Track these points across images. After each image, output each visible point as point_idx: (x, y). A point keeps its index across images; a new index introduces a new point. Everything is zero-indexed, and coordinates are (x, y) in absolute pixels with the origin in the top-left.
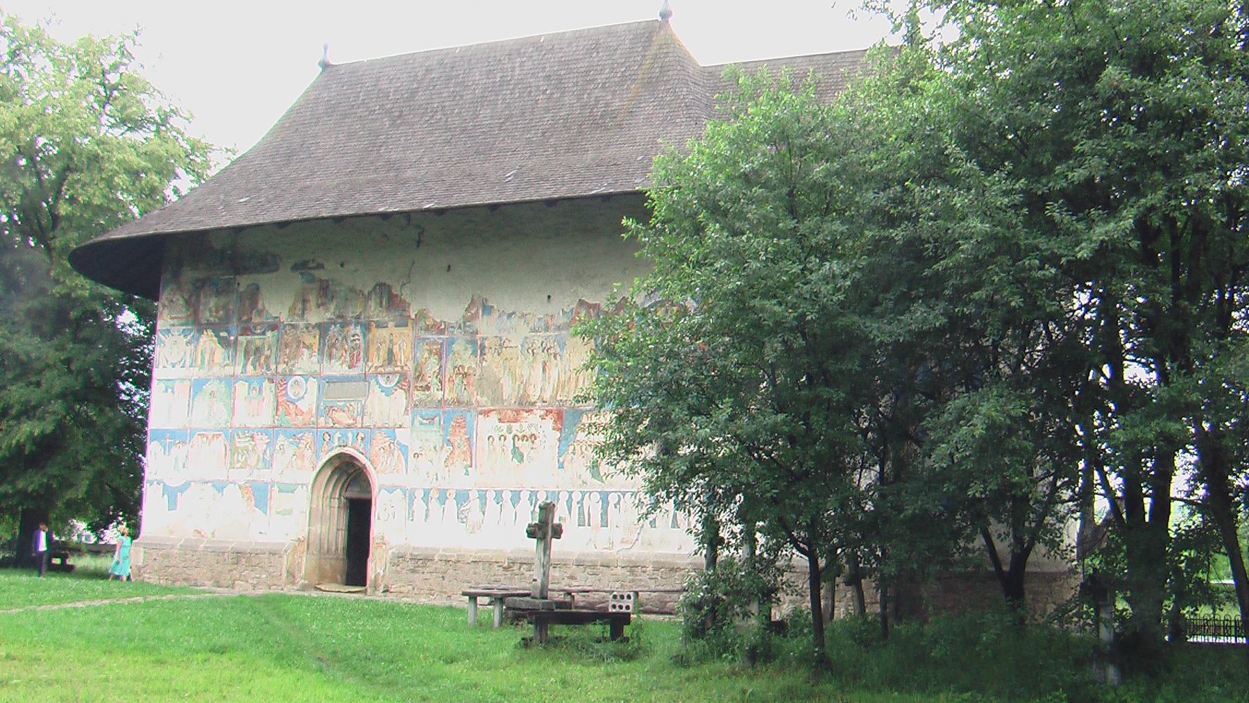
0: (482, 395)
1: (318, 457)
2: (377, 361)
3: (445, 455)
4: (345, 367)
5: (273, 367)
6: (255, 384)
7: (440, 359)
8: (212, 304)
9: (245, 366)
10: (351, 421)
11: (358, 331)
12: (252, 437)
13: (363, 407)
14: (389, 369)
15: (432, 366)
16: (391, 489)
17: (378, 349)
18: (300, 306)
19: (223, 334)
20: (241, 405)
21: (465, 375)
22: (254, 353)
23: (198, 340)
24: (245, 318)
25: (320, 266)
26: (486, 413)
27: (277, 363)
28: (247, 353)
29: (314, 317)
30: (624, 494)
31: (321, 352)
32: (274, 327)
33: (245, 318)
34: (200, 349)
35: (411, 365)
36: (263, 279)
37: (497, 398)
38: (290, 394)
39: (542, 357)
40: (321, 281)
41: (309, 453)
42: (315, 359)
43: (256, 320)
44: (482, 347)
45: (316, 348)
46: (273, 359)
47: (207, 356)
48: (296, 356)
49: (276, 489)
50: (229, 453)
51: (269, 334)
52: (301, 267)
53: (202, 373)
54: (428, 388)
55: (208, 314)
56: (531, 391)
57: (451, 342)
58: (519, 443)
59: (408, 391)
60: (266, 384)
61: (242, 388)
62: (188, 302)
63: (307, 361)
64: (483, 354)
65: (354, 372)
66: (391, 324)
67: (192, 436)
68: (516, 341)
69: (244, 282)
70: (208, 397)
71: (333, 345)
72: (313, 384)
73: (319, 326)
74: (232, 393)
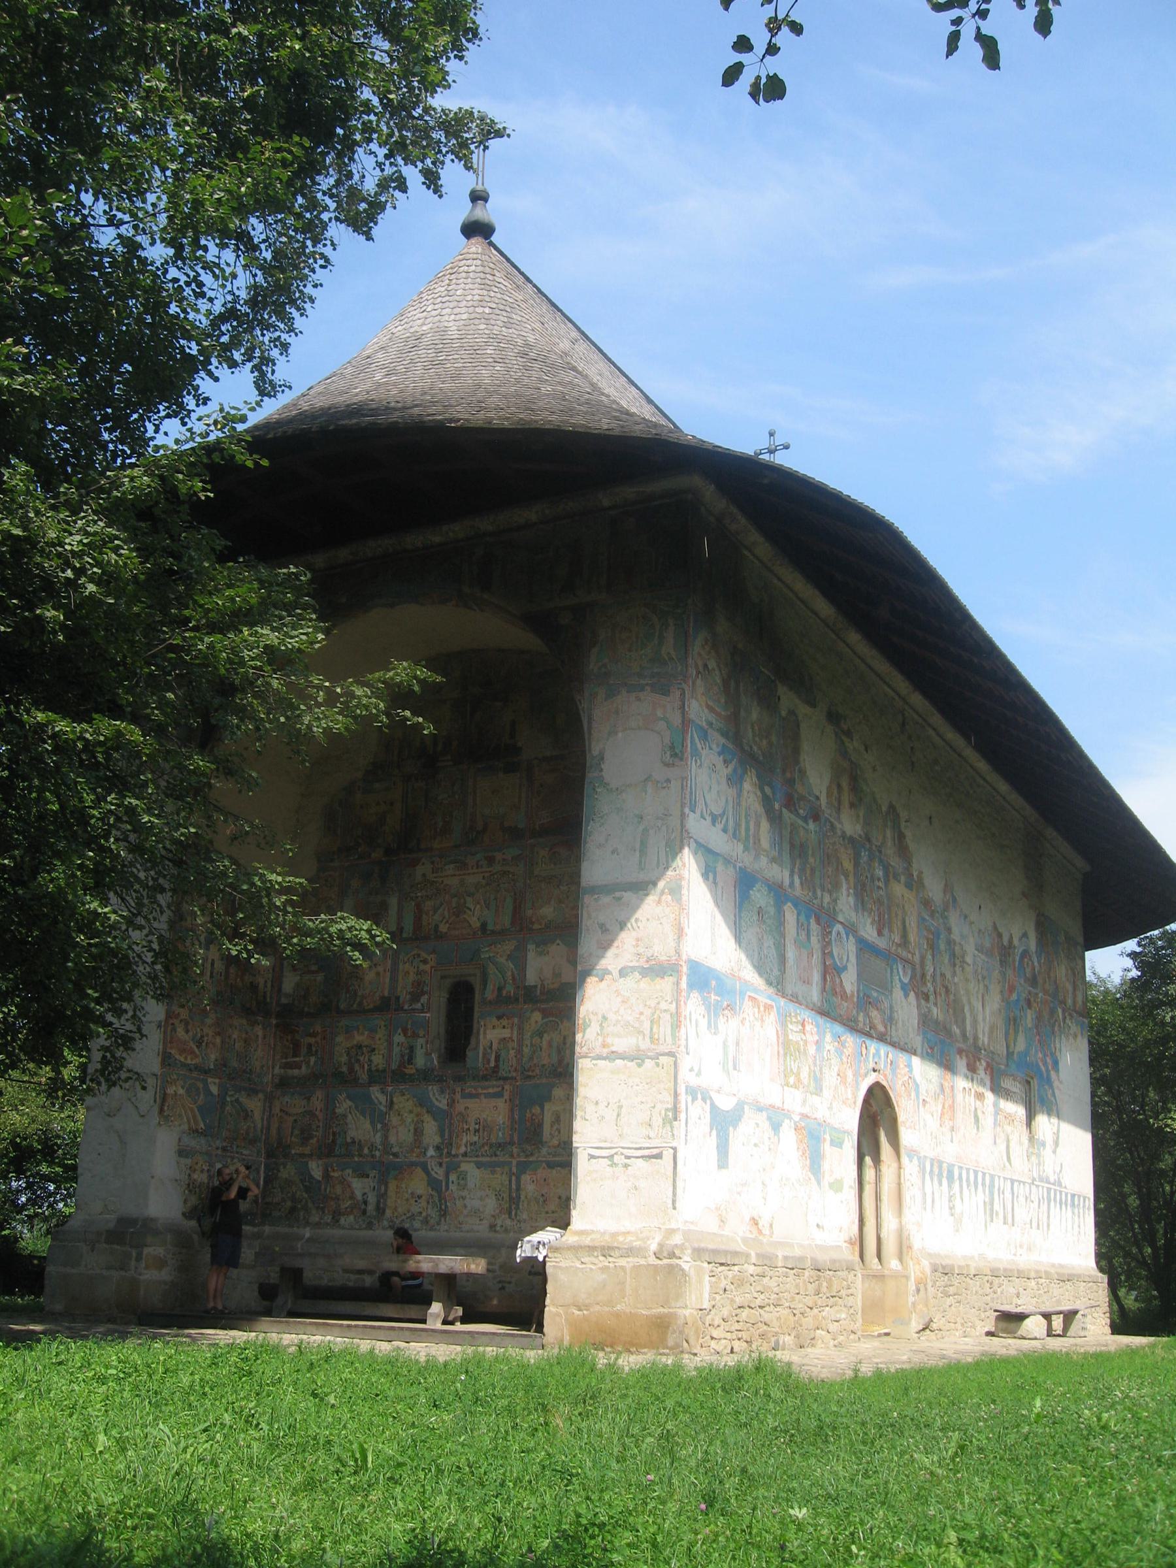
0: (956, 1022)
1: (857, 1089)
2: (897, 939)
3: (940, 1107)
4: (875, 934)
5: (819, 893)
6: (802, 918)
7: (933, 956)
8: (755, 715)
9: (791, 876)
10: (881, 1028)
11: (881, 873)
12: (803, 1025)
13: (891, 1007)
14: (904, 954)
15: (930, 969)
16: (913, 1153)
17: (897, 915)
18: (835, 792)
19: (767, 789)
20: (791, 954)
21: (947, 991)
22: (796, 850)
23: (741, 780)
24: (788, 775)
25: (848, 734)
26: (960, 1052)
27: (823, 890)
28: (792, 845)
29: (850, 825)
30: (1020, 1182)
31: (856, 895)
32: (816, 818)
33: (788, 775)
34: (744, 803)
35: (917, 959)
36: (803, 709)
37: (964, 1035)
38: (835, 954)
39: (981, 986)
40: (852, 762)
41: (850, 1074)
42: (851, 900)
43: (799, 788)
44: (954, 955)
45: (851, 878)
46: (817, 873)
47: (752, 827)
48: (837, 886)
49: (827, 1137)
50: (782, 1052)
51: (812, 826)
52: (833, 717)
53: (747, 860)
54: (927, 999)
55: (750, 734)
56: (981, 1036)
57: (938, 938)
58: (978, 1103)
59: (917, 995)
60: (812, 921)
61: (790, 915)
62: (726, 683)
63: (846, 903)
64: (955, 965)
65: (882, 943)
66: (903, 878)
67: (742, 994)
68: (969, 959)
69: (787, 699)
70: (755, 918)
71: (864, 885)
72: (851, 946)
73: (852, 840)
74: (781, 922)
